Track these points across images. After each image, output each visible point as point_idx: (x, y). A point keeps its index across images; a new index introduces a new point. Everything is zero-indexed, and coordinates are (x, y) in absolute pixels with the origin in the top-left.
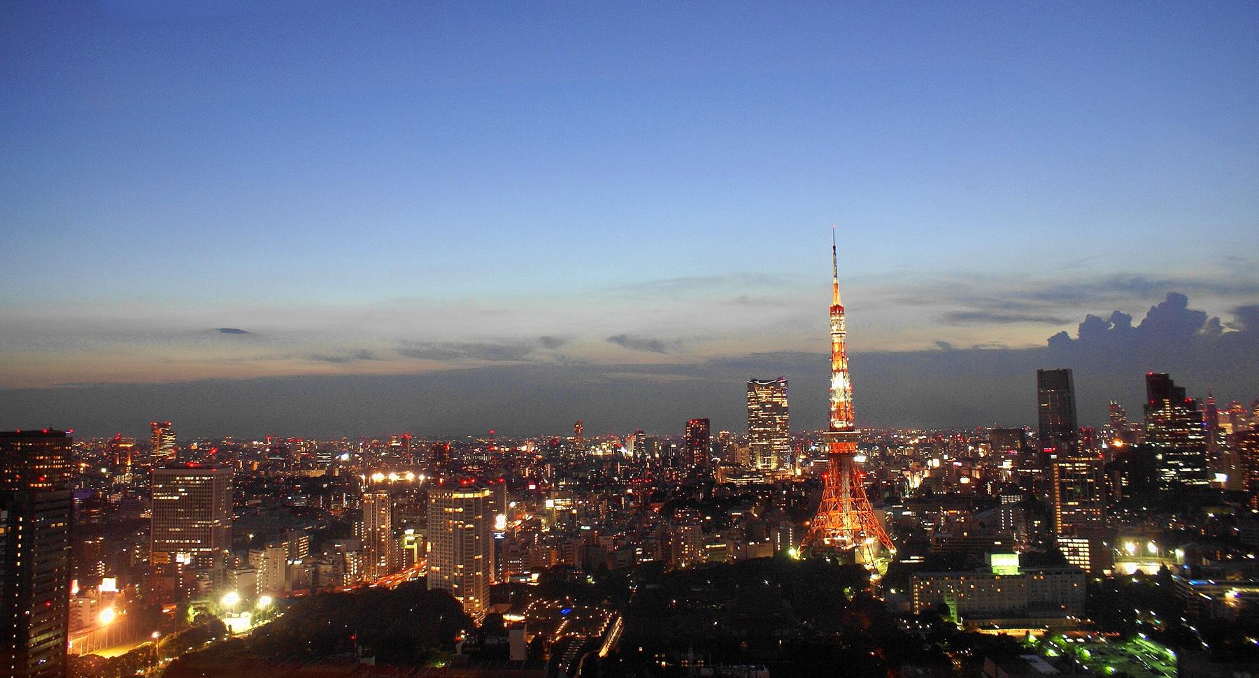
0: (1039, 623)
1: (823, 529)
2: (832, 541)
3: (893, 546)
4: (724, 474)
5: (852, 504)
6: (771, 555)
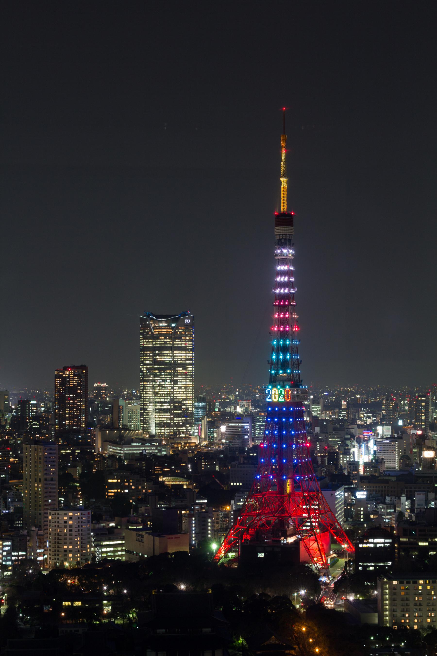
4: (106, 441)
6: (187, 549)
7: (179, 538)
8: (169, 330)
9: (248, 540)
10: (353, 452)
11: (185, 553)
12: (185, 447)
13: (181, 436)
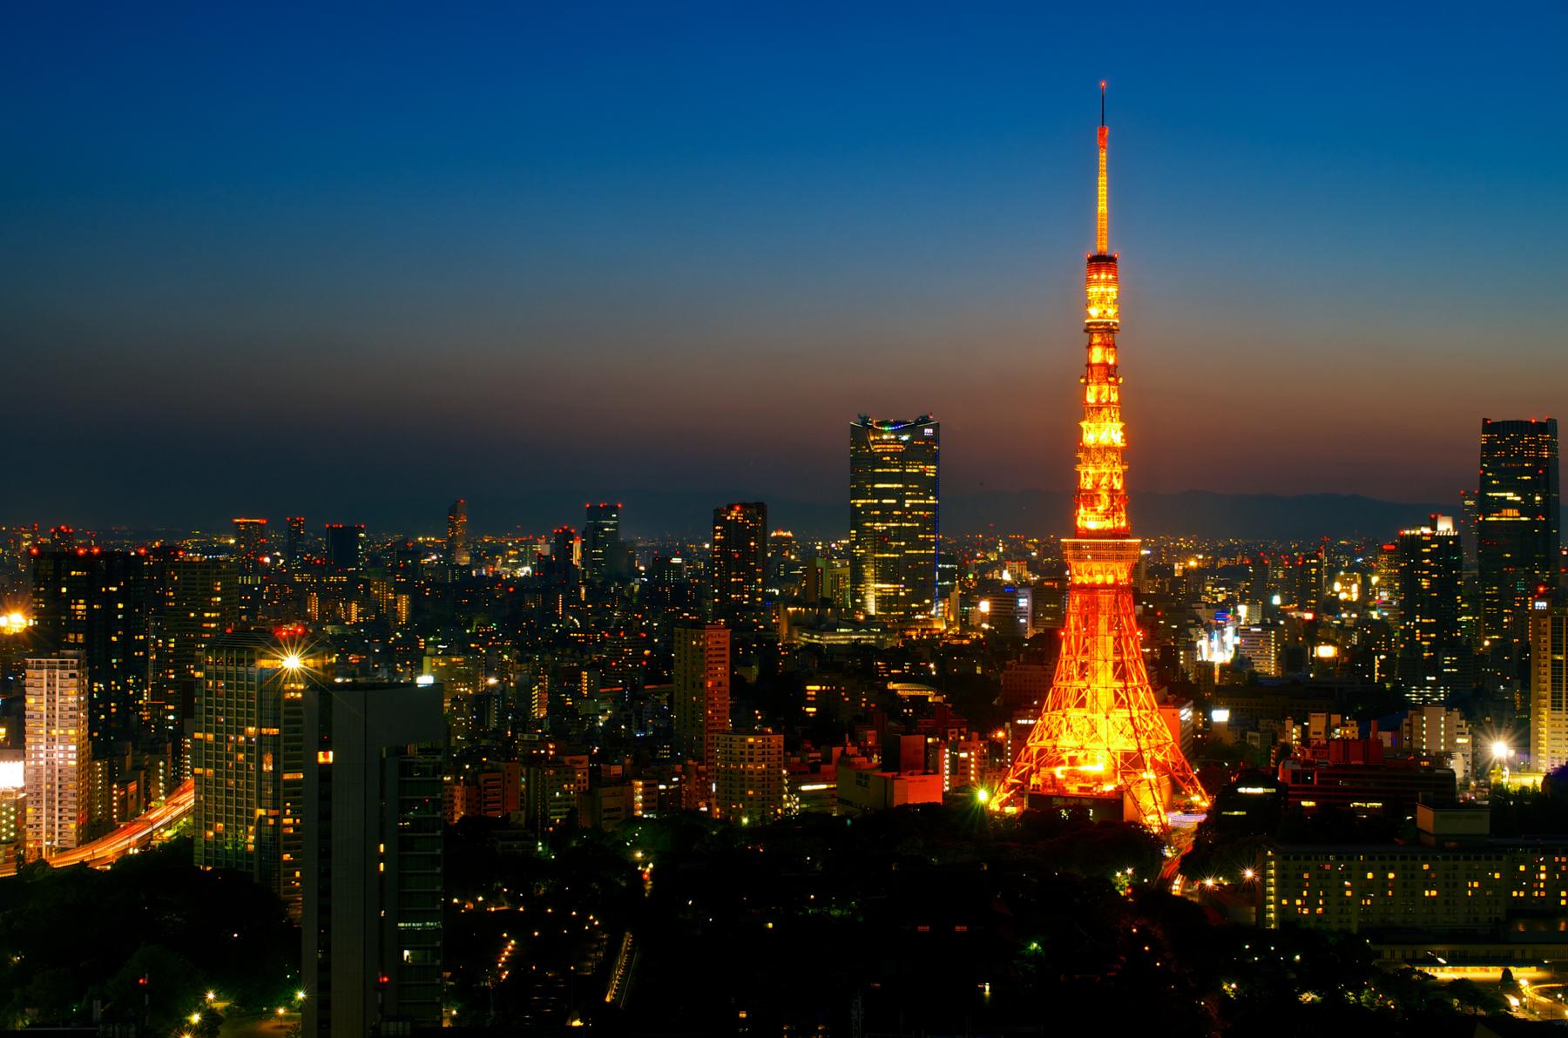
0: (1529, 955)
1: (1055, 747)
2: (1073, 775)
3: (1200, 788)
4: (795, 624)
5: (1115, 692)
6: (939, 800)
8: (898, 446)
9: (1038, 786)
10: (1201, 646)
11: (939, 803)
12: (923, 635)
13: (916, 617)
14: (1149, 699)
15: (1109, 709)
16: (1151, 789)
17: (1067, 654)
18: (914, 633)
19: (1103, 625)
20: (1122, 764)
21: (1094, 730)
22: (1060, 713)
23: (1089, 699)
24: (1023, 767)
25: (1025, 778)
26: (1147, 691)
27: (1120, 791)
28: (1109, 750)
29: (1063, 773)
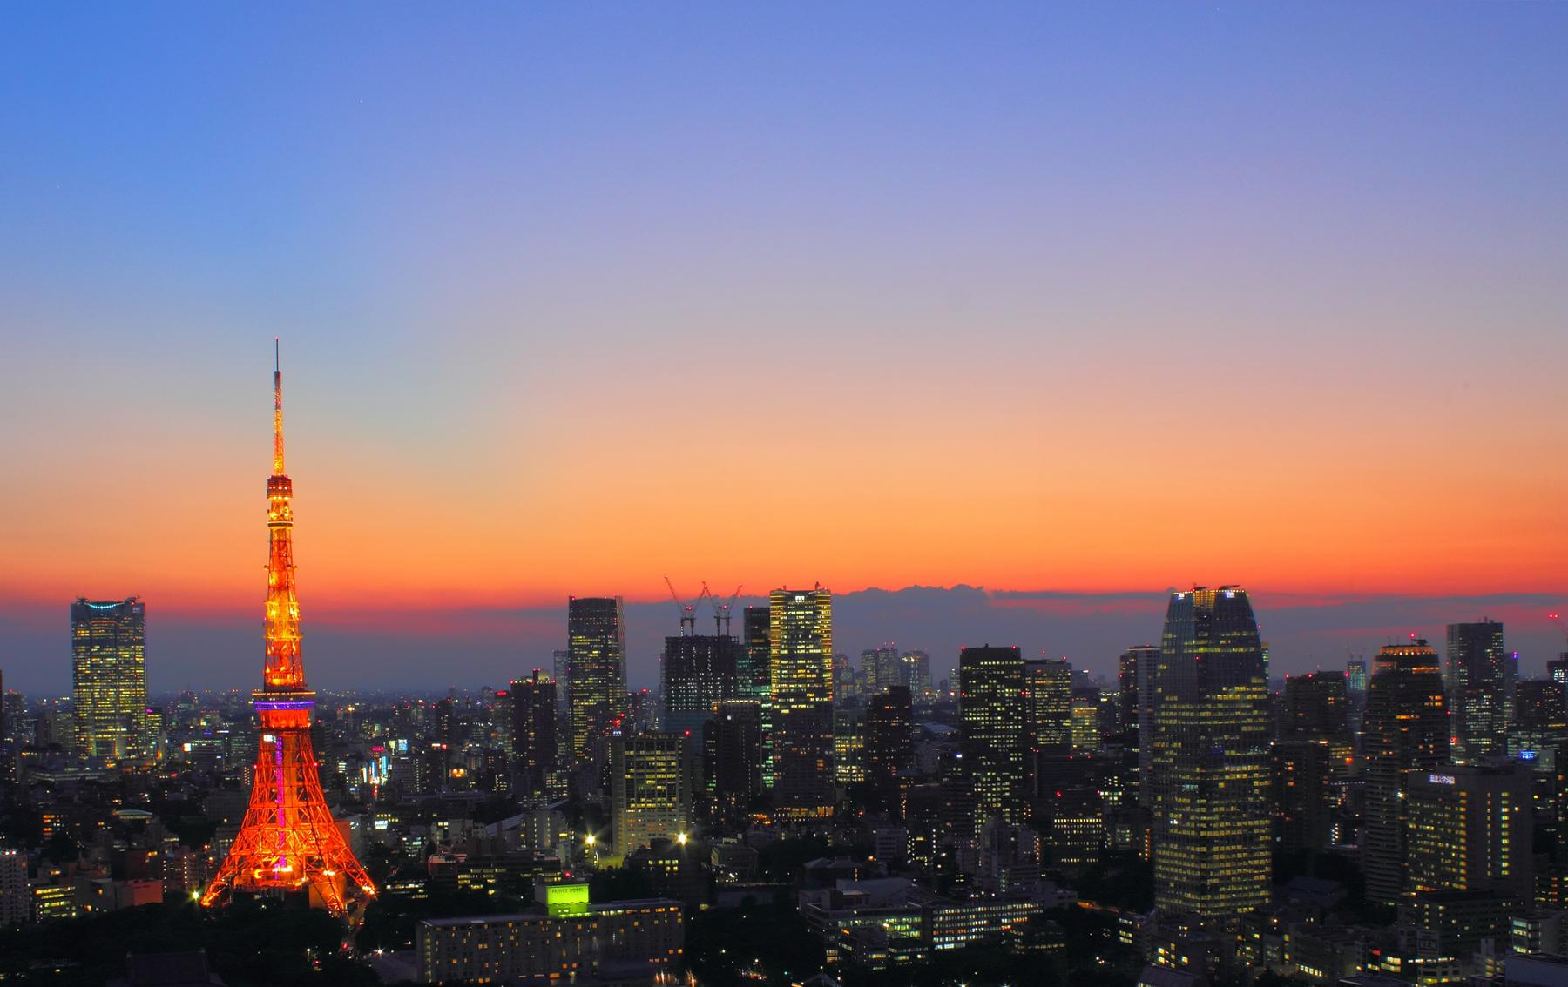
1: (253, 855)
2: (268, 876)
3: (368, 881)
7: (148, 886)
14: (327, 816)
15: (296, 823)
16: (331, 884)
17: (260, 782)
18: (130, 770)
19: (288, 759)
20: (307, 866)
21: (283, 837)
22: (256, 828)
23: (278, 820)
24: (228, 872)
25: (231, 881)
26: (324, 808)
27: (306, 886)
28: (296, 855)
29: (260, 874)
